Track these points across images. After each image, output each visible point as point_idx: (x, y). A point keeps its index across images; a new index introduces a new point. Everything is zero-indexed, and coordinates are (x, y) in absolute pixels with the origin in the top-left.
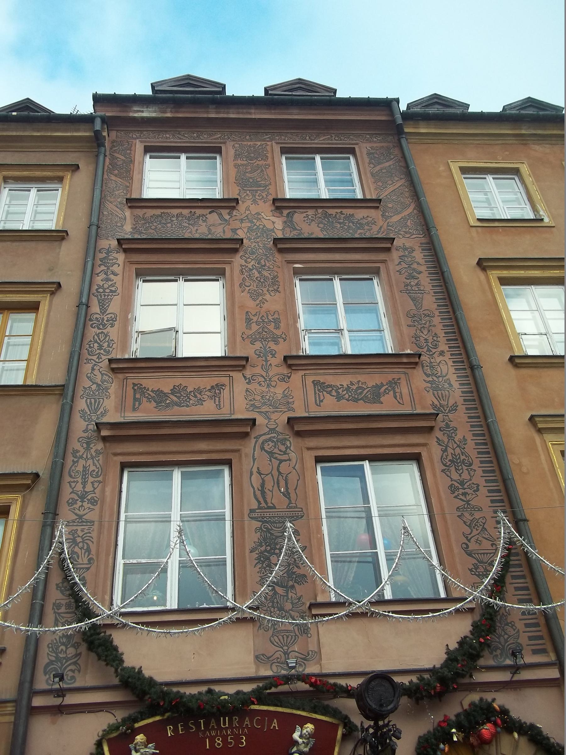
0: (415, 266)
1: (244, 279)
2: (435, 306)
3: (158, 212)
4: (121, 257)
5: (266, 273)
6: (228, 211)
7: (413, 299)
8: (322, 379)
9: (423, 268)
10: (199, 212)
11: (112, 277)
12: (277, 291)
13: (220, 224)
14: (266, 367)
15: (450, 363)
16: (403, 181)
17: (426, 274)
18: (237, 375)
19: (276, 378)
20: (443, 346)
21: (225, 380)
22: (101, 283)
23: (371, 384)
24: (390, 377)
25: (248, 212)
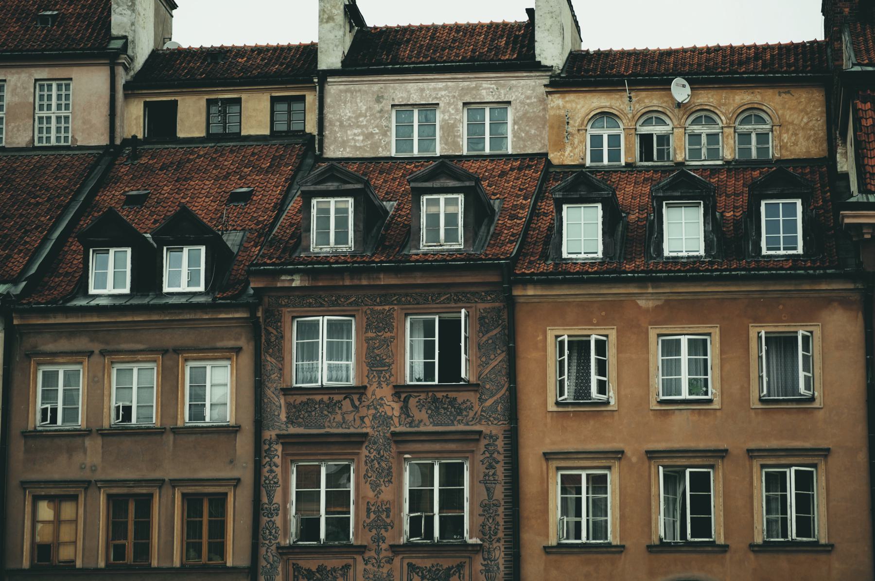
0: (495, 455)
1: (367, 471)
2: (502, 496)
3: (304, 398)
4: (279, 448)
5: (383, 464)
6: (358, 396)
7: (488, 489)
8: (414, 561)
9: (501, 458)
10: (337, 398)
11: (274, 468)
12: (390, 481)
13: (352, 412)
14: (378, 552)
15: (502, 549)
16: (504, 354)
17: (502, 464)
18: (359, 558)
19: (383, 561)
20: (501, 534)
21: (351, 561)
22: (267, 475)
23: (445, 566)
24: (458, 561)
25: (374, 397)
